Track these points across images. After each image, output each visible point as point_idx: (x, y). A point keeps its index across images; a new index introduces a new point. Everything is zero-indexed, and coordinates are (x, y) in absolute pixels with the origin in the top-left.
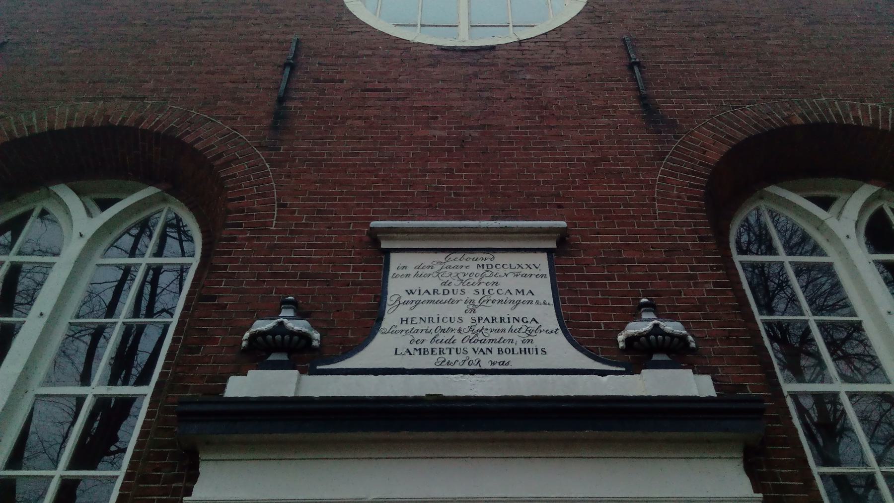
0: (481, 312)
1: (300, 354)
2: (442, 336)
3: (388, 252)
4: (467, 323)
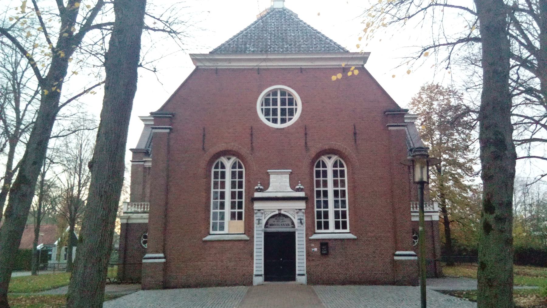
1: (261, 190)
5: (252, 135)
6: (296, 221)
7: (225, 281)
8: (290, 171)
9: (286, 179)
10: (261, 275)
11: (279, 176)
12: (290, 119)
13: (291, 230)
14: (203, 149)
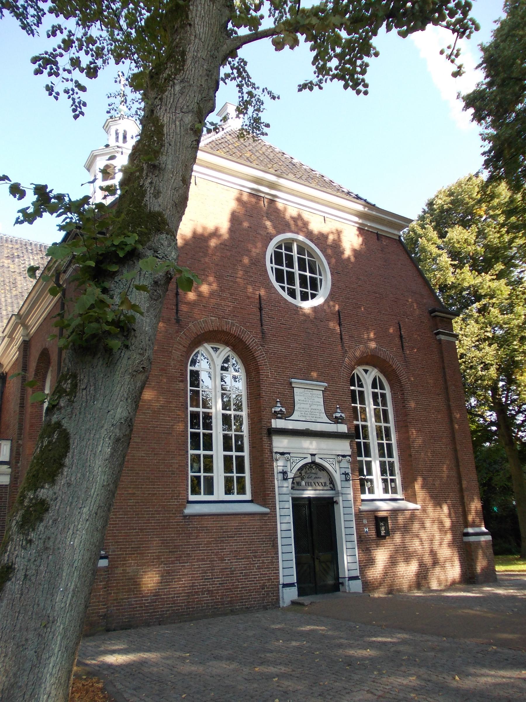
0: (312, 407)
1: (284, 416)
2: (306, 413)
3: (293, 387)
4: (310, 410)
5: (261, 309)
6: (338, 477)
7: (230, 602)
8: (326, 384)
9: (318, 398)
10: (291, 585)
11: (309, 392)
12: (313, 296)
13: (328, 494)
14: (178, 321)
